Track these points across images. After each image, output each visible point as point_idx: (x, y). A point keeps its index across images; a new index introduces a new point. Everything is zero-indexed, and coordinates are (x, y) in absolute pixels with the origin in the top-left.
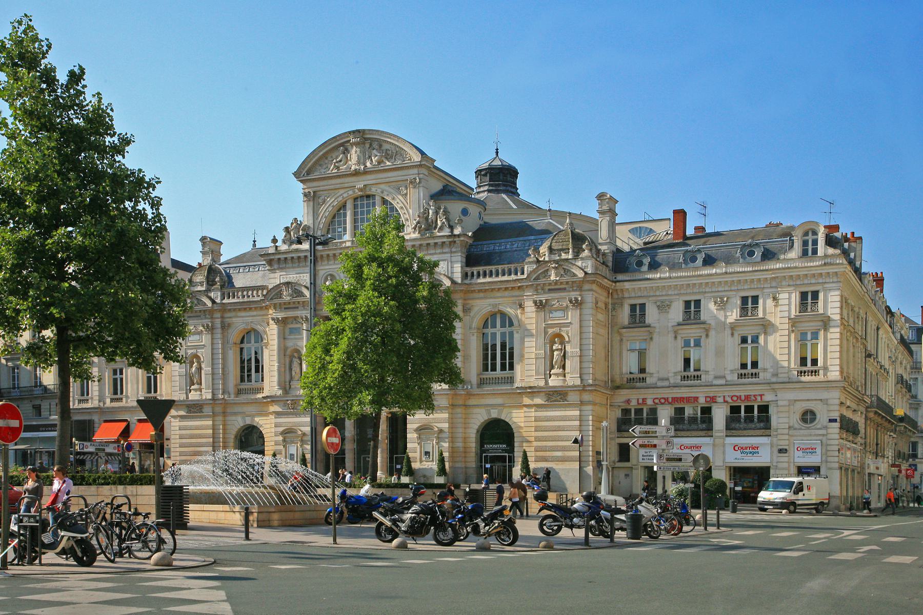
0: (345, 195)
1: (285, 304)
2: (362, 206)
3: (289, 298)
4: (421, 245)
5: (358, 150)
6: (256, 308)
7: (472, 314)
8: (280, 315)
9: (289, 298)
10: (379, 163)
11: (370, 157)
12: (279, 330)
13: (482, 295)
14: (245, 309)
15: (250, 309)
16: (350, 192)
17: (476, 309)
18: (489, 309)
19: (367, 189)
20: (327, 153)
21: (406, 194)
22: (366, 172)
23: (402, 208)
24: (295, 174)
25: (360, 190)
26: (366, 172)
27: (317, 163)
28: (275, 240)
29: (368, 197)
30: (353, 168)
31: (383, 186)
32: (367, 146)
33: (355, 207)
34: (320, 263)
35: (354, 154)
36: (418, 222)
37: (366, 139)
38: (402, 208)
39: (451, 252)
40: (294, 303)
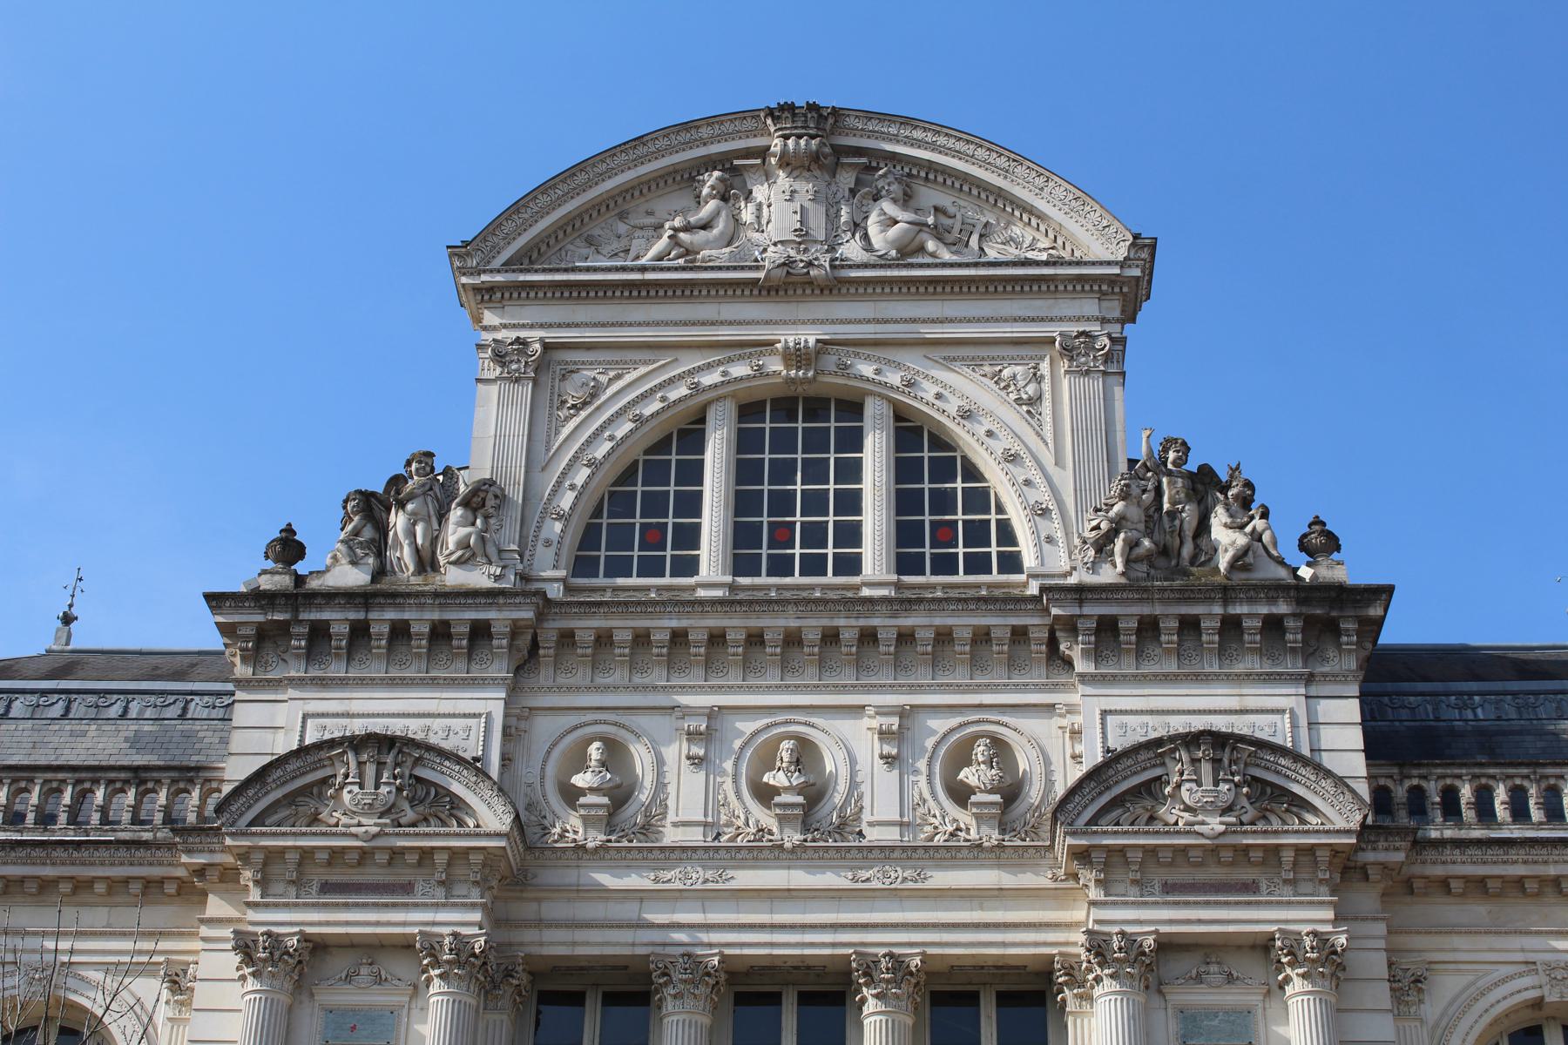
0: (708, 379)
1: (336, 854)
2: (783, 441)
3: (371, 825)
4: (1149, 628)
5: (805, 188)
6: (116, 886)
7: (1431, 1009)
8: (295, 919)
9: (371, 825)
10: (908, 250)
11: (857, 226)
12: (270, 1007)
13: (1479, 911)
14: (46, 886)
15: (81, 886)
16: (740, 370)
17: (1447, 987)
18: (1525, 988)
19: (830, 362)
20: (627, 192)
21: (1034, 401)
22: (837, 285)
23: (1012, 458)
24: (459, 252)
25: (796, 357)
26: (837, 285)
27: (572, 226)
28: (288, 548)
29: (816, 407)
30: (774, 255)
31: (913, 360)
32: (846, 179)
33: (746, 441)
34: (545, 676)
35: (776, 211)
36: (1117, 525)
37: (840, 151)
38: (1012, 458)
39: (1309, 679)
40: (396, 854)
